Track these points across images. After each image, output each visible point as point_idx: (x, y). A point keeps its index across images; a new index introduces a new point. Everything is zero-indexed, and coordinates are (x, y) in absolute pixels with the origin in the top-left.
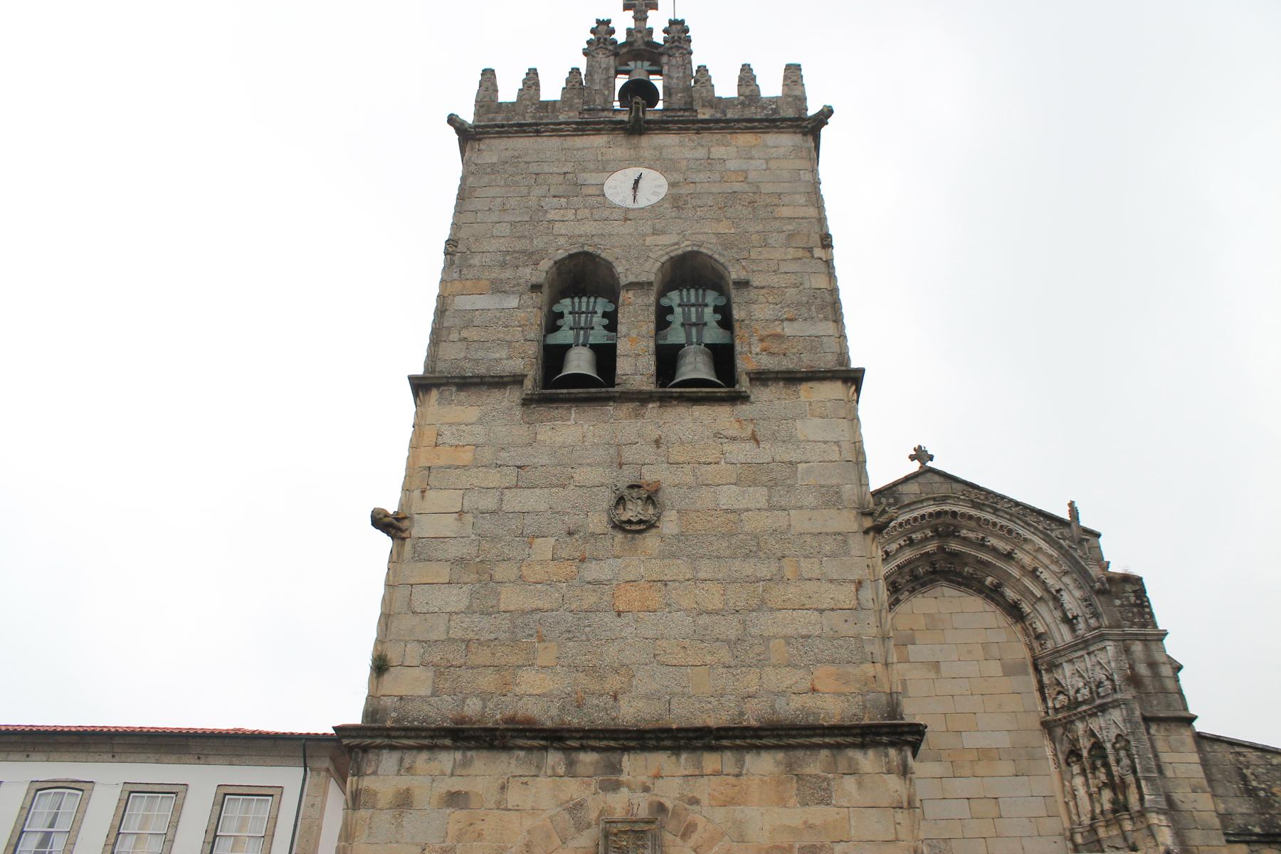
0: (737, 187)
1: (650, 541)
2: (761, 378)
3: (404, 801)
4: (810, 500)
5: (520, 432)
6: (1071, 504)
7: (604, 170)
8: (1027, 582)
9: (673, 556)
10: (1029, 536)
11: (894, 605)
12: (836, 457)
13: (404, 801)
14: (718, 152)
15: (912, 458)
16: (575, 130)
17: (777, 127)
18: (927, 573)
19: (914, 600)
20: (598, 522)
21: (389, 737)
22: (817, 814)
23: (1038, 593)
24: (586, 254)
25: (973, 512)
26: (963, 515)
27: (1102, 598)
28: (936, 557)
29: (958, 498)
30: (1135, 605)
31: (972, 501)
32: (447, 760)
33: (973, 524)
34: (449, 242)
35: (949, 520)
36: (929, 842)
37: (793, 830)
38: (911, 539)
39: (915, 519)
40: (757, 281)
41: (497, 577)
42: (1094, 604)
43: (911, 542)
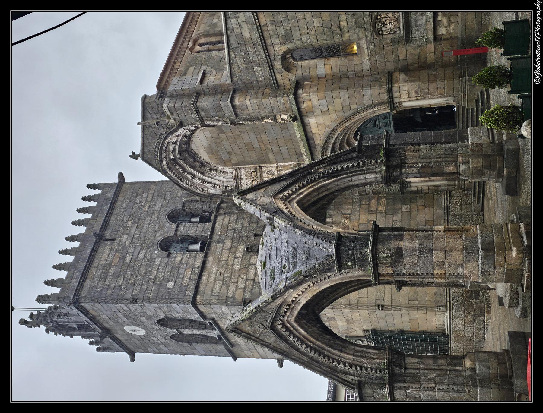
11: (207, 163)
15: (137, 159)
16: (116, 340)
34: (180, 355)
38: (183, 172)
39: (176, 176)
43: (185, 170)
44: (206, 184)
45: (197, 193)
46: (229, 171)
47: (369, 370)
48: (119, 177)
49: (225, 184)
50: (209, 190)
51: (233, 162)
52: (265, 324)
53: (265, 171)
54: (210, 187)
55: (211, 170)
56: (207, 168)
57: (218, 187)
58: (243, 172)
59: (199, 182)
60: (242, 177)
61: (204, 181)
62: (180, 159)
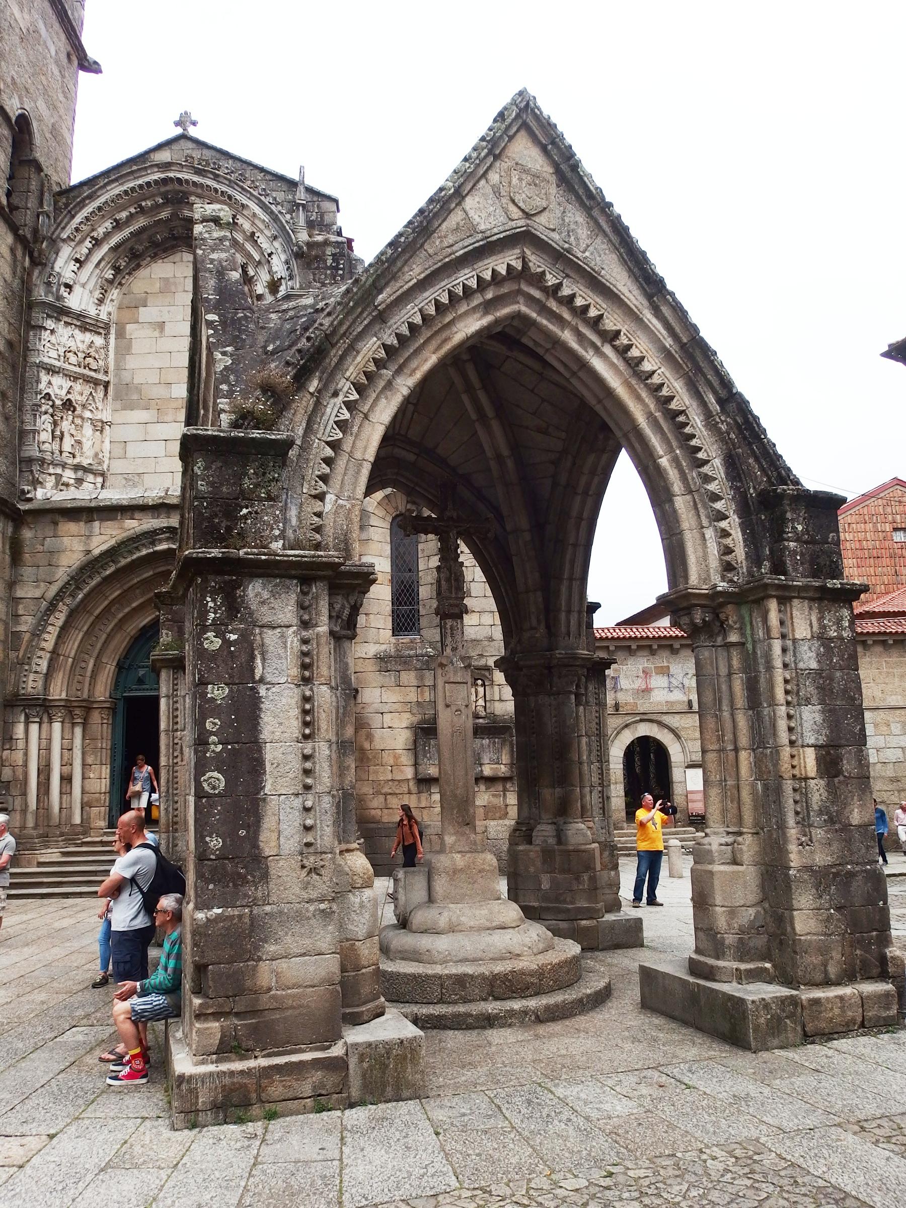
6: (301, 169)
8: (248, 247)
10: (245, 201)
15: (177, 124)
18: (165, 240)
19: (154, 265)
23: (257, 257)
25: (196, 178)
26: (187, 181)
27: (299, 261)
28: (173, 224)
29: (180, 164)
30: (331, 267)
31: (194, 167)
33: (199, 191)
35: (177, 187)
36: (126, 476)
38: (140, 206)
39: (141, 186)
42: (291, 267)
43: (142, 211)
44: (90, 246)
45: (76, 213)
46: (102, 308)
47: (317, 506)
48: (95, 63)
49: (77, 289)
50: (73, 244)
51: (128, 327)
52: (542, 219)
53: (96, 392)
54: (78, 249)
55: (117, 270)
56: (124, 264)
57: (76, 270)
58: (99, 341)
59: (100, 231)
60: (88, 337)
61: (97, 243)
62: (174, 215)
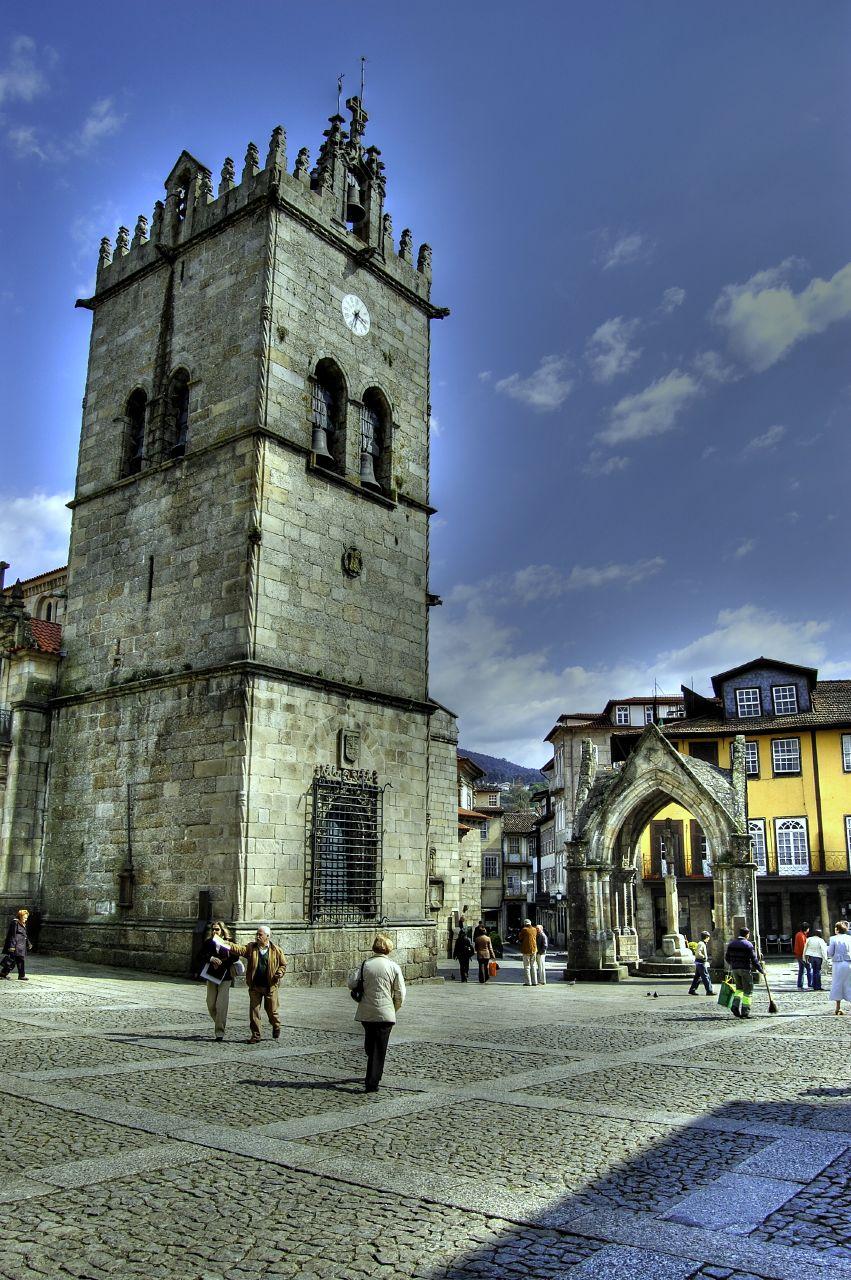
0: (399, 345)
1: (356, 582)
2: (402, 499)
3: (271, 705)
4: (411, 580)
5: (307, 489)
7: (342, 288)
9: (364, 594)
12: (421, 558)
13: (271, 705)
14: (394, 308)
17: (420, 304)
20: (338, 565)
21: (267, 671)
22: (404, 738)
24: (331, 360)
32: (285, 687)
37: (396, 743)
40: (404, 426)
41: (301, 584)
